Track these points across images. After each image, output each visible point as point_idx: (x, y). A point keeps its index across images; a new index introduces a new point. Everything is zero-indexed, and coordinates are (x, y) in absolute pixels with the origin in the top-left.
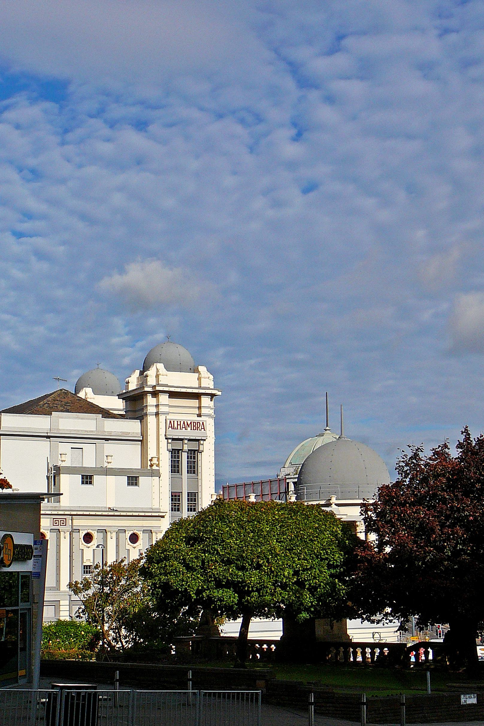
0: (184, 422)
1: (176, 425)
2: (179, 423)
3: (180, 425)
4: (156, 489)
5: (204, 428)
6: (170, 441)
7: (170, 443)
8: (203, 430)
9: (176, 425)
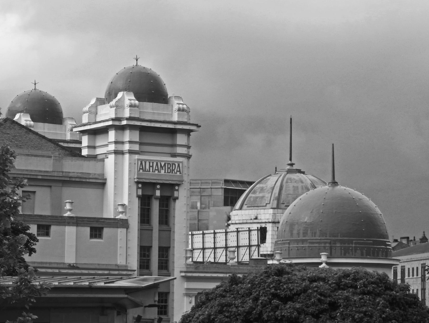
1: (147, 167)
5: (180, 171)
6: (140, 186)
9: (147, 167)
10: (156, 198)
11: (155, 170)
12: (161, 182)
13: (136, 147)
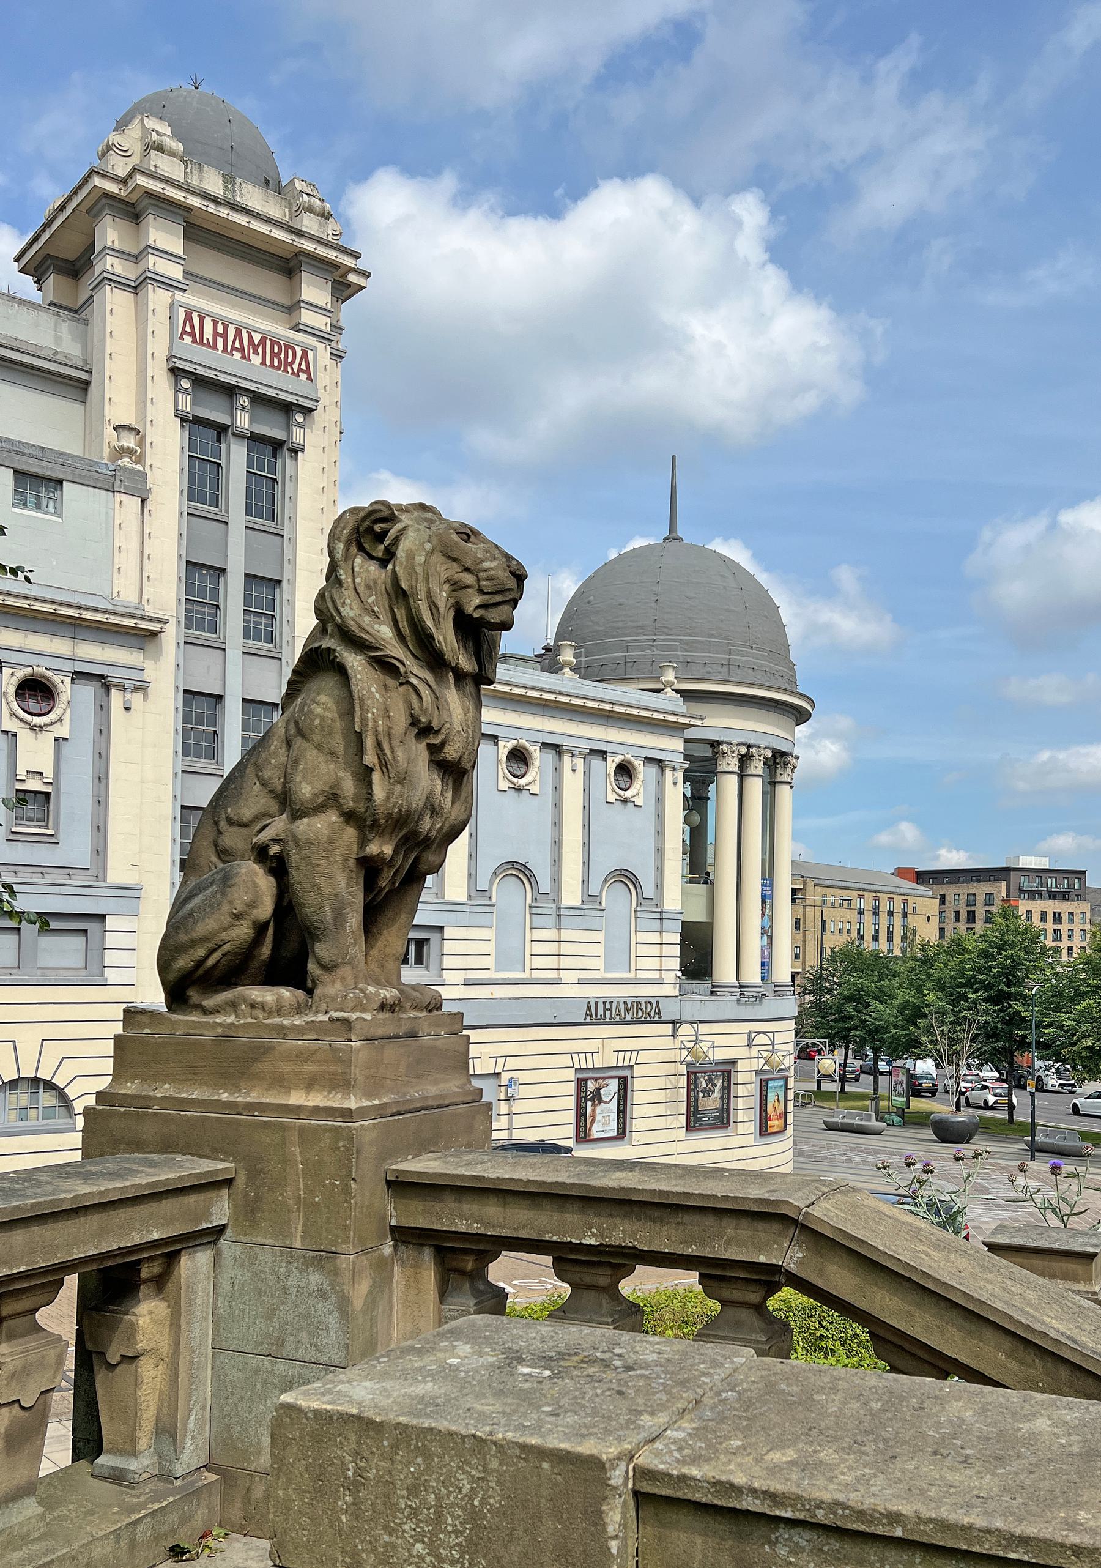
2: (220, 330)
3: (225, 336)
4: (127, 539)
5: (307, 371)
6: (186, 384)
7: (184, 391)
8: (303, 376)
10: (238, 436)
11: (233, 348)
12: (252, 387)
13: (175, 272)
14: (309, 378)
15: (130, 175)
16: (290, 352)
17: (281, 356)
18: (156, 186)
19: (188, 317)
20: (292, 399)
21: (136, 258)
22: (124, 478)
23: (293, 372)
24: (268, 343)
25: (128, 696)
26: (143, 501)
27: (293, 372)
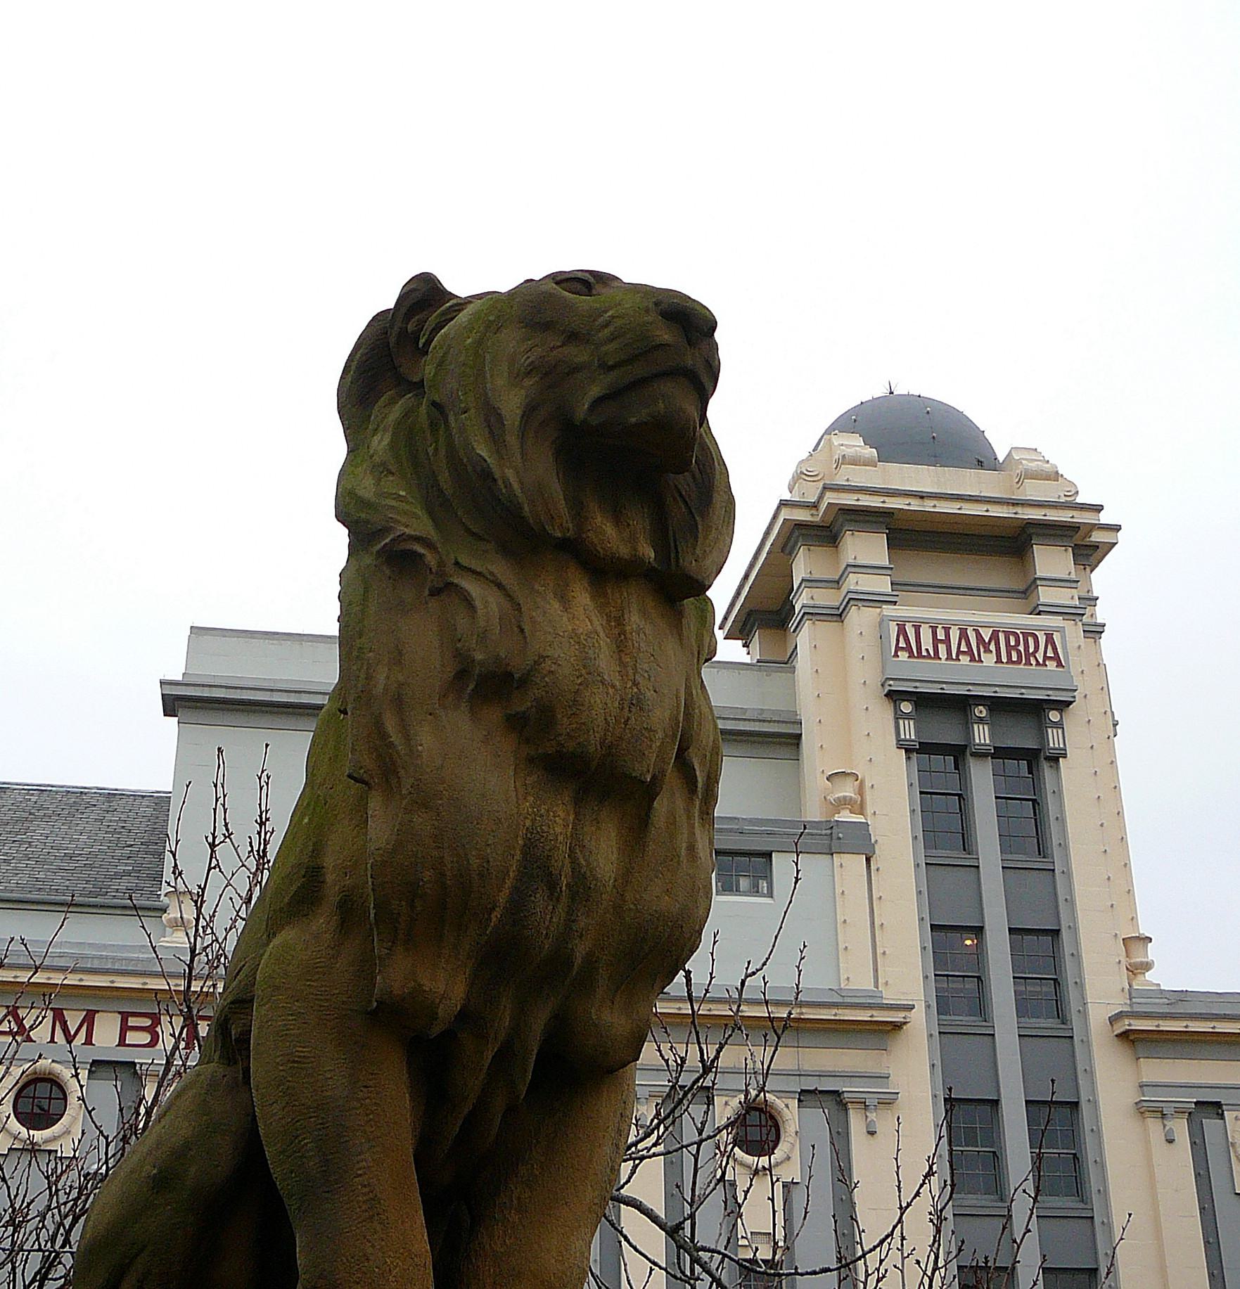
0: (963, 634)
1: (927, 643)
2: (941, 635)
3: (947, 641)
4: (854, 908)
5: (1056, 658)
6: (906, 707)
7: (907, 716)
8: (1051, 665)
9: (927, 643)
11: (959, 652)
12: (987, 692)
13: (883, 585)
14: (1060, 664)
15: (821, 497)
16: (1031, 640)
17: (1019, 647)
18: (849, 500)
19: (902, 630)
20: (1041, 695)
21: (837, 583)
22: (841, 838)
23: (1038, 663)
24: (1001, 636)
25: (872, 1116)
26: (868, 860)
27: (1038, 663)
